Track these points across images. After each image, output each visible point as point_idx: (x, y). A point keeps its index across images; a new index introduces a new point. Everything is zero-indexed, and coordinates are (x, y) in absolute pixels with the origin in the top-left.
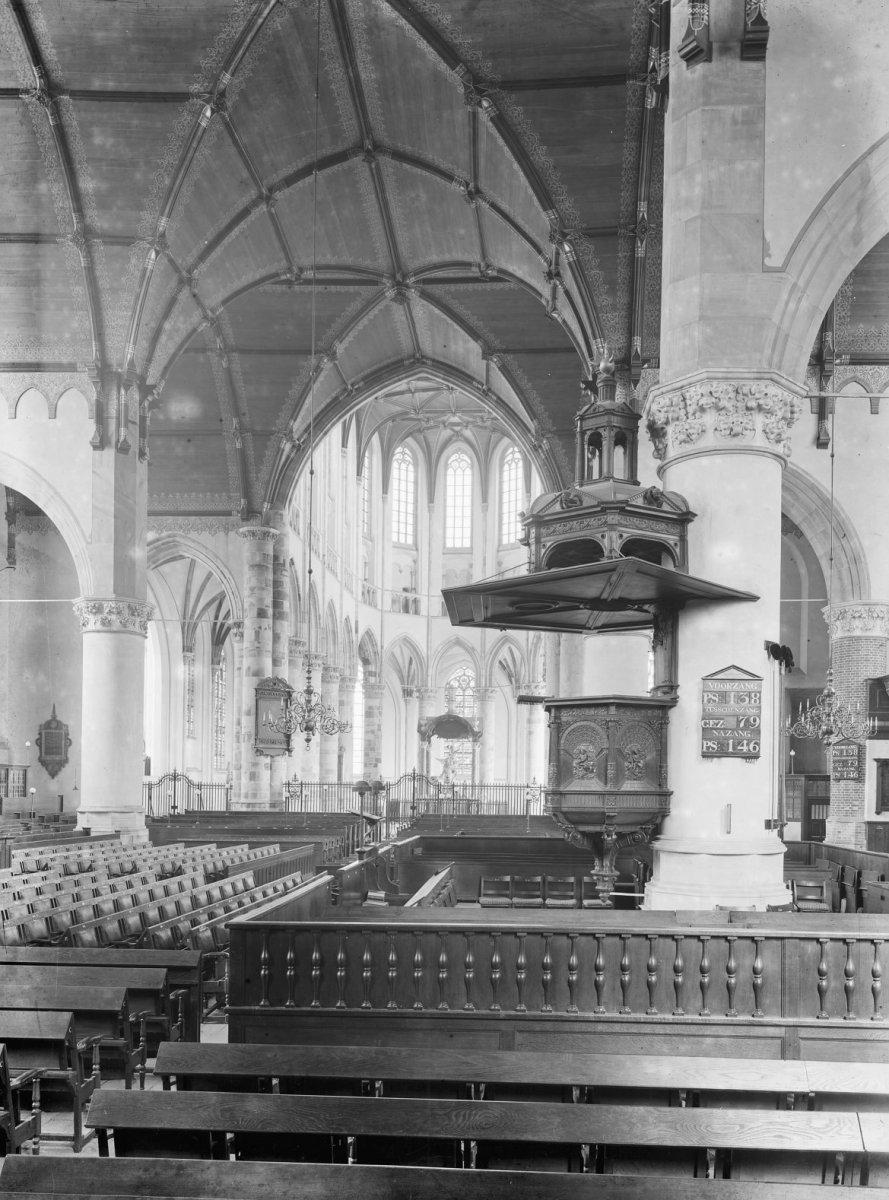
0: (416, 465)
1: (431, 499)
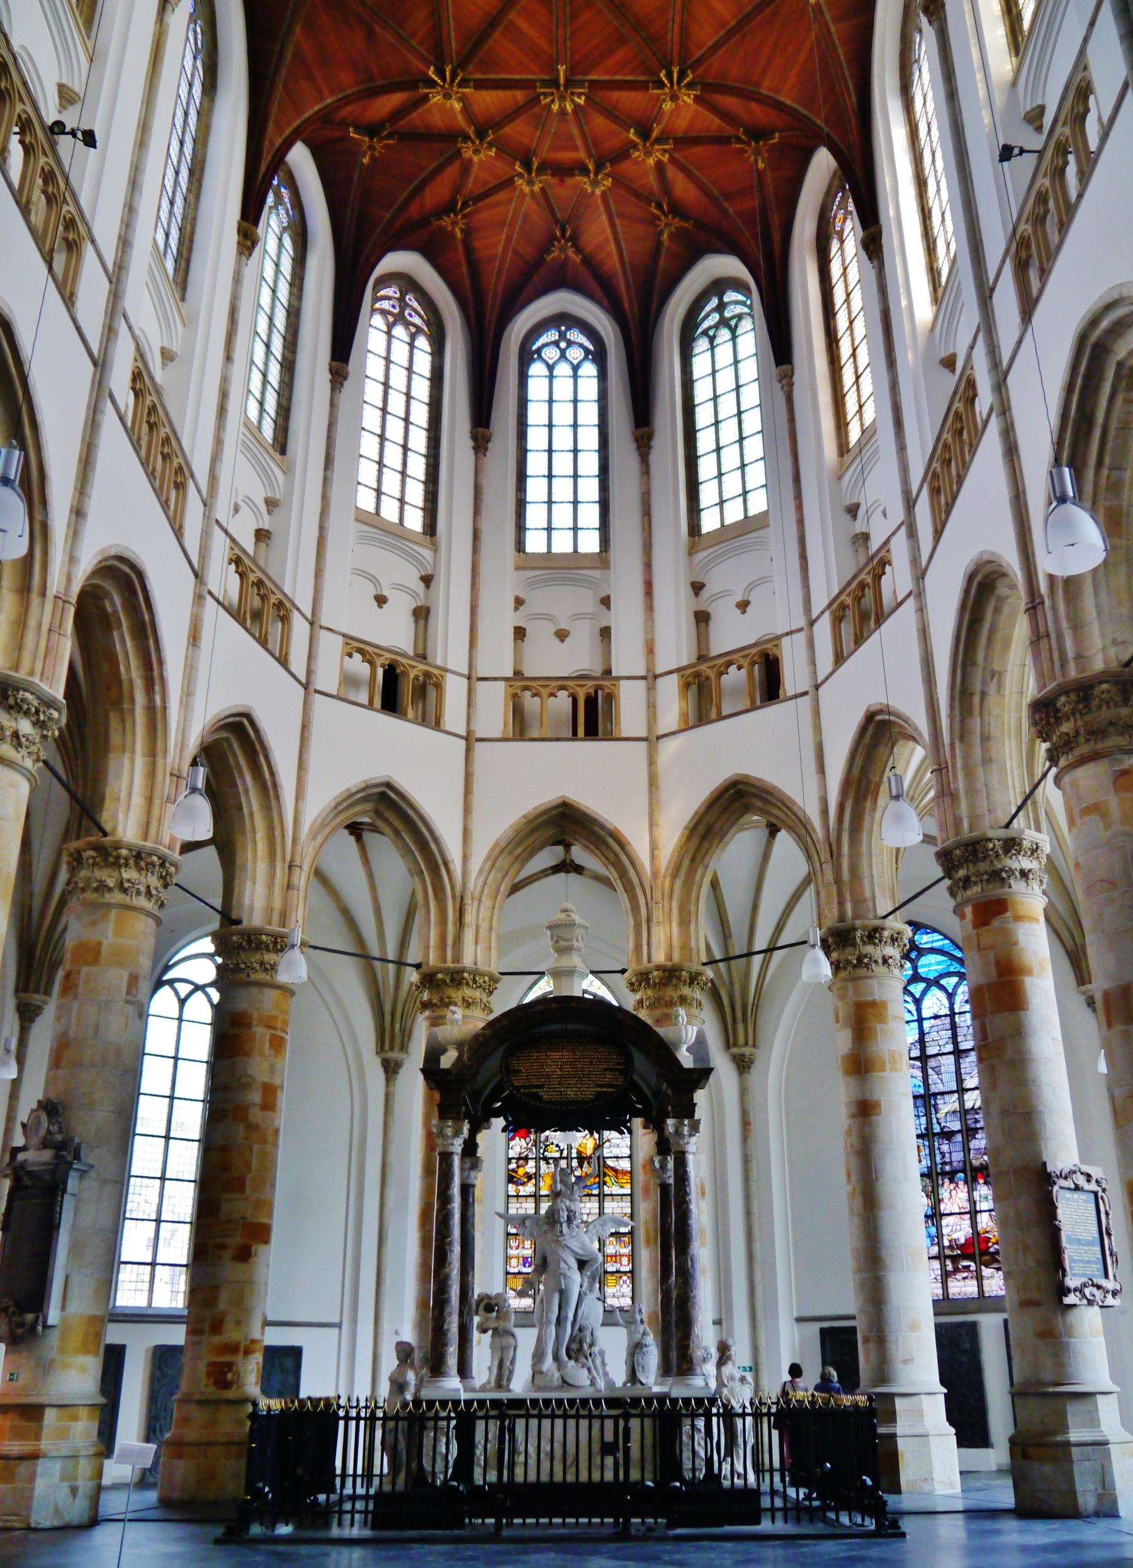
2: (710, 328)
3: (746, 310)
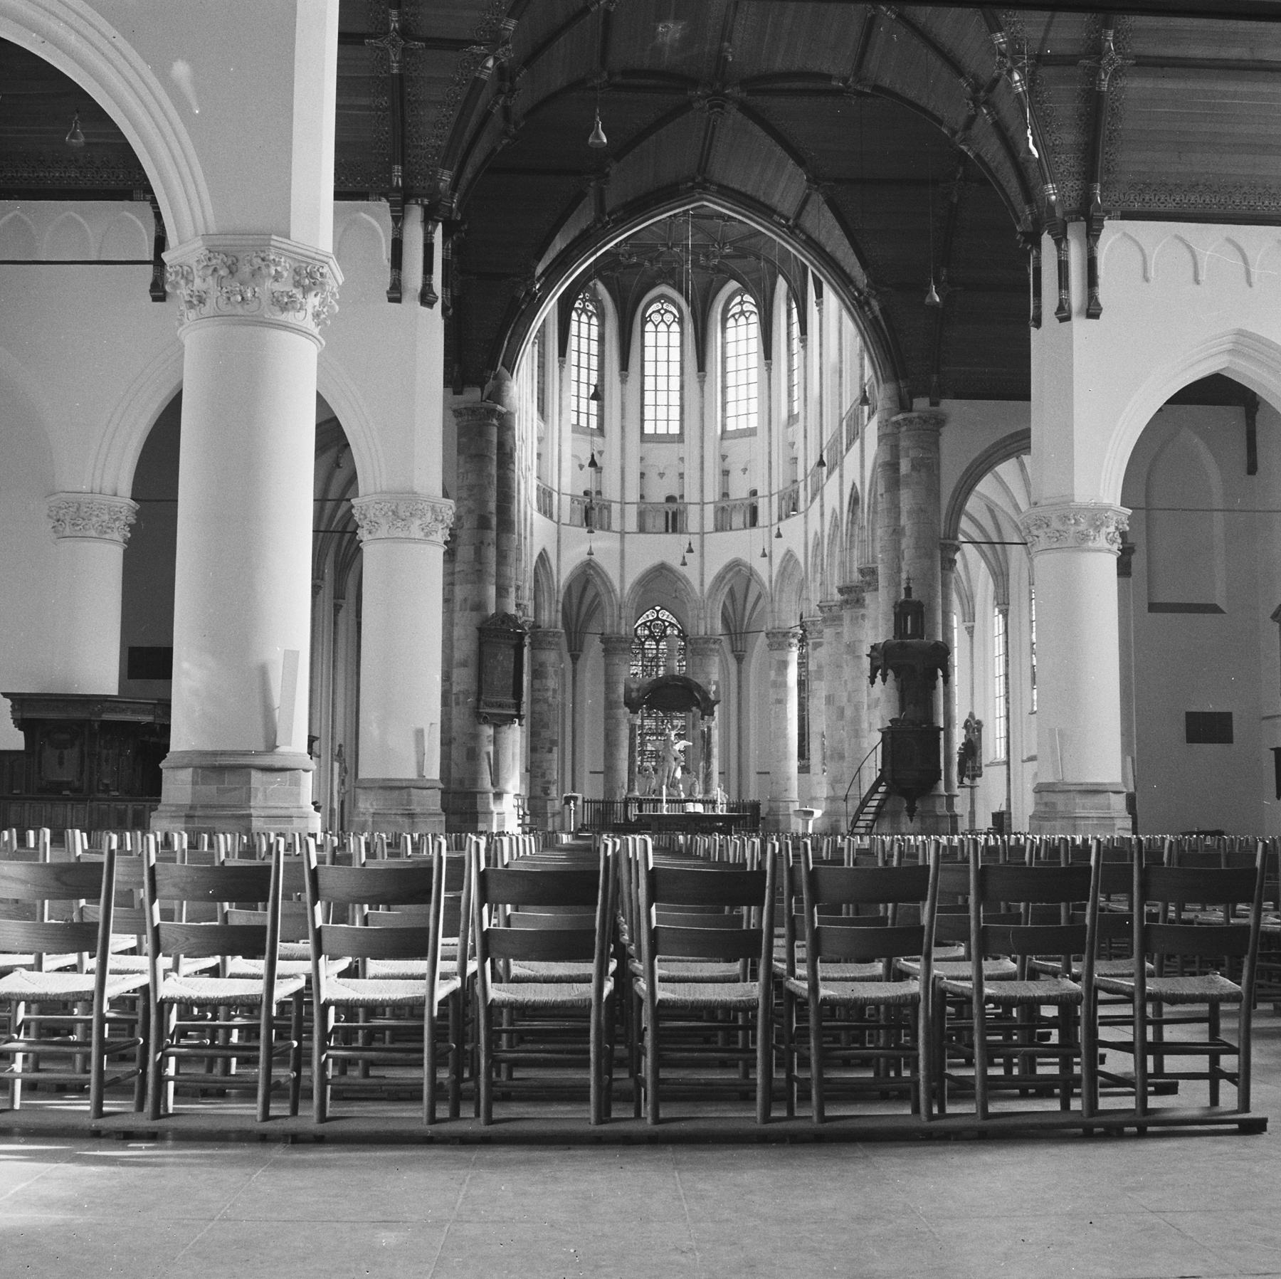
0: (601, 316)
1: (624, 365)
3: (756, 310)
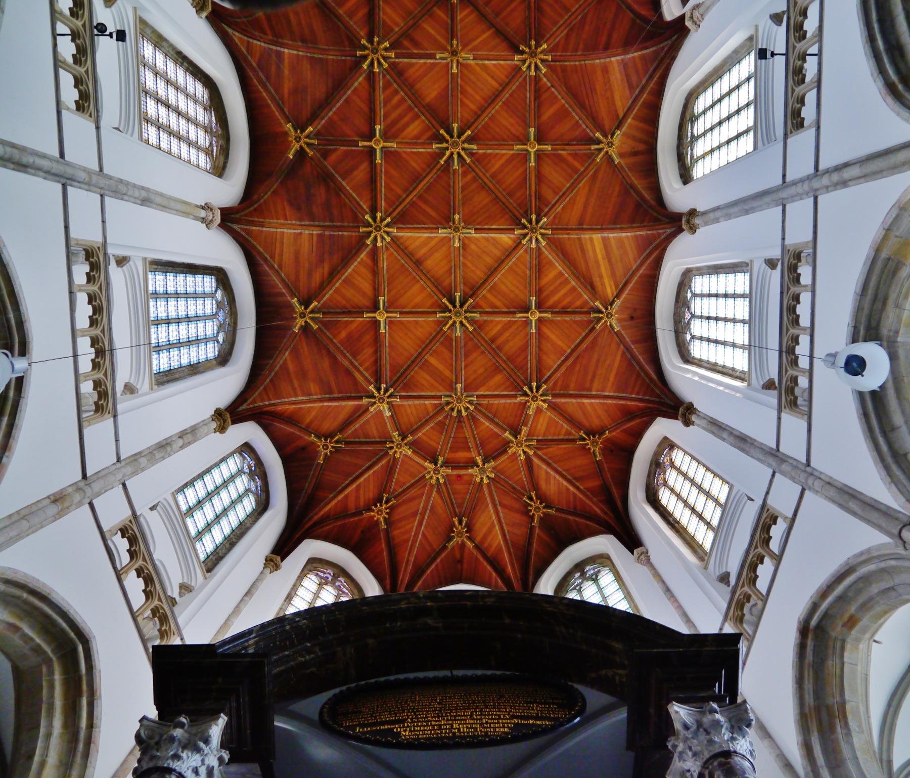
2: (577, 585)
